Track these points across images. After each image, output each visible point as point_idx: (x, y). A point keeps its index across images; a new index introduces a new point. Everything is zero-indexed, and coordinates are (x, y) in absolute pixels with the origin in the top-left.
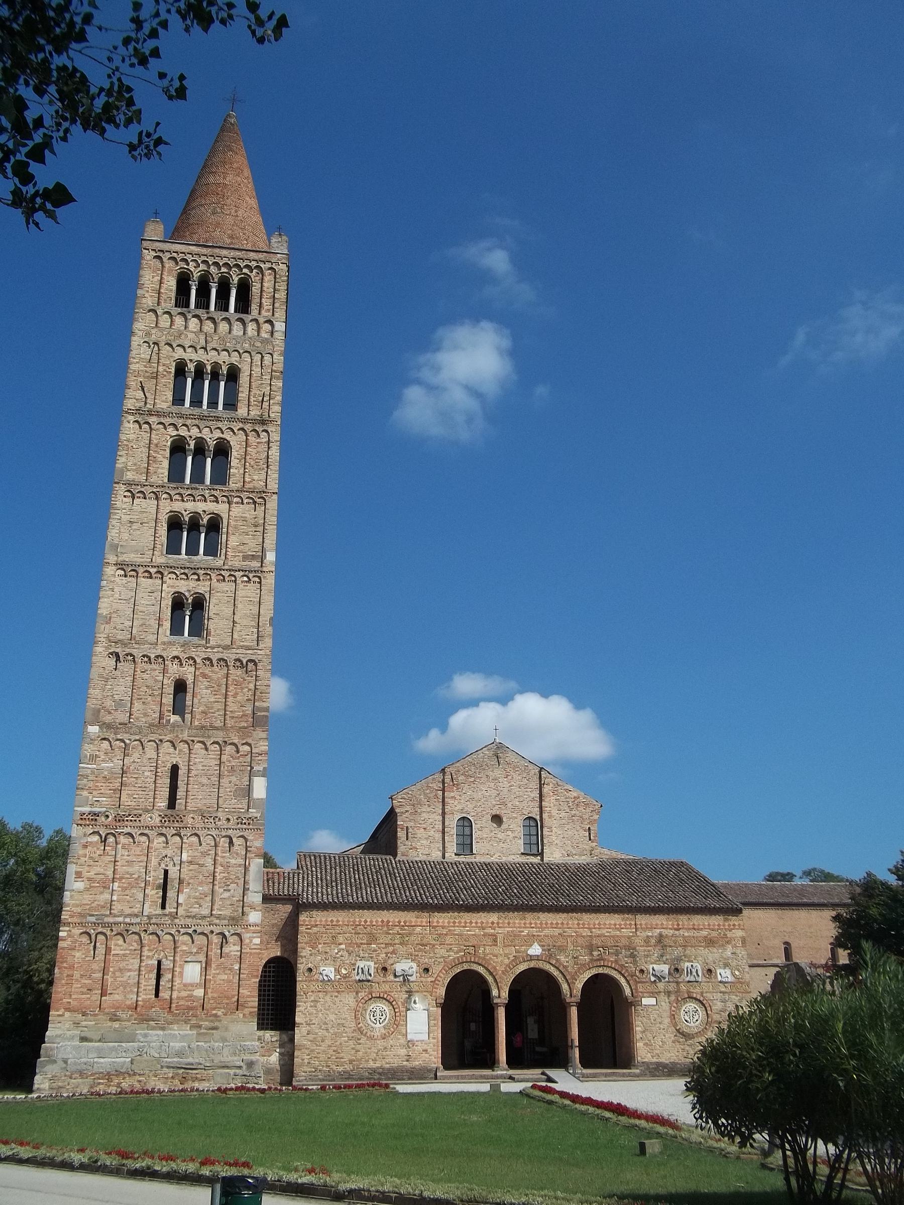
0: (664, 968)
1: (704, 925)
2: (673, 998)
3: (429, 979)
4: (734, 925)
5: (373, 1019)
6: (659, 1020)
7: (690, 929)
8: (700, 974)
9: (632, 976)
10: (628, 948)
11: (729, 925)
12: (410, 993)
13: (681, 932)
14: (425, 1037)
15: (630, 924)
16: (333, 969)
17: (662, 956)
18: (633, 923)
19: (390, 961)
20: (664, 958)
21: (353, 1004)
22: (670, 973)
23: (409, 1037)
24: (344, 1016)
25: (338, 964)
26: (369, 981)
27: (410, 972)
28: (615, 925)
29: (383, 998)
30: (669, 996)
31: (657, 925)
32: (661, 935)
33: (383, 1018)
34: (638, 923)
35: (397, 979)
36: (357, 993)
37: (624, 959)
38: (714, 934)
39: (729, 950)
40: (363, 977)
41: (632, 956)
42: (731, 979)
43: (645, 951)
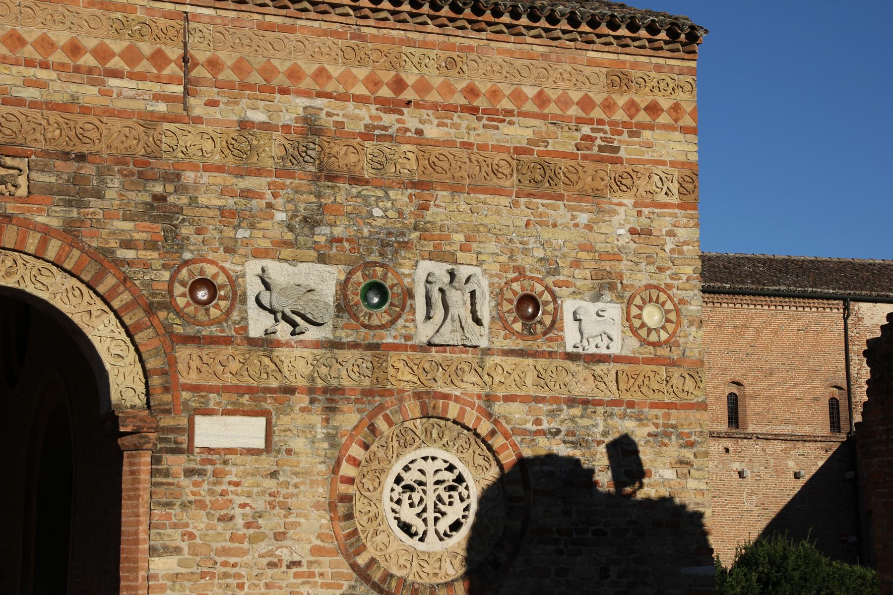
0: (325, 280)
1: (518, 96)
2: (349, 419)
4: (653, 109)
6: (271, 523)
7: (452, 109)
8: (485, 311)
9: (150, 309)
10: (141, 168)
11: (632, 107)
13: (411, 119)
15: (159, 59)
17: (311, 222)
18: (174, 52)
20: (322, 234)
22: (343, 307)
28: (75, 49)
30: (331, 410)
31: (294, 74)
32: (311, 127)
34: (201, 55)
37: (115, 219)
38: (565, 141)
39: (619, 224)
41: (159, 210)
42: (621, 344)
43: (224, 191)
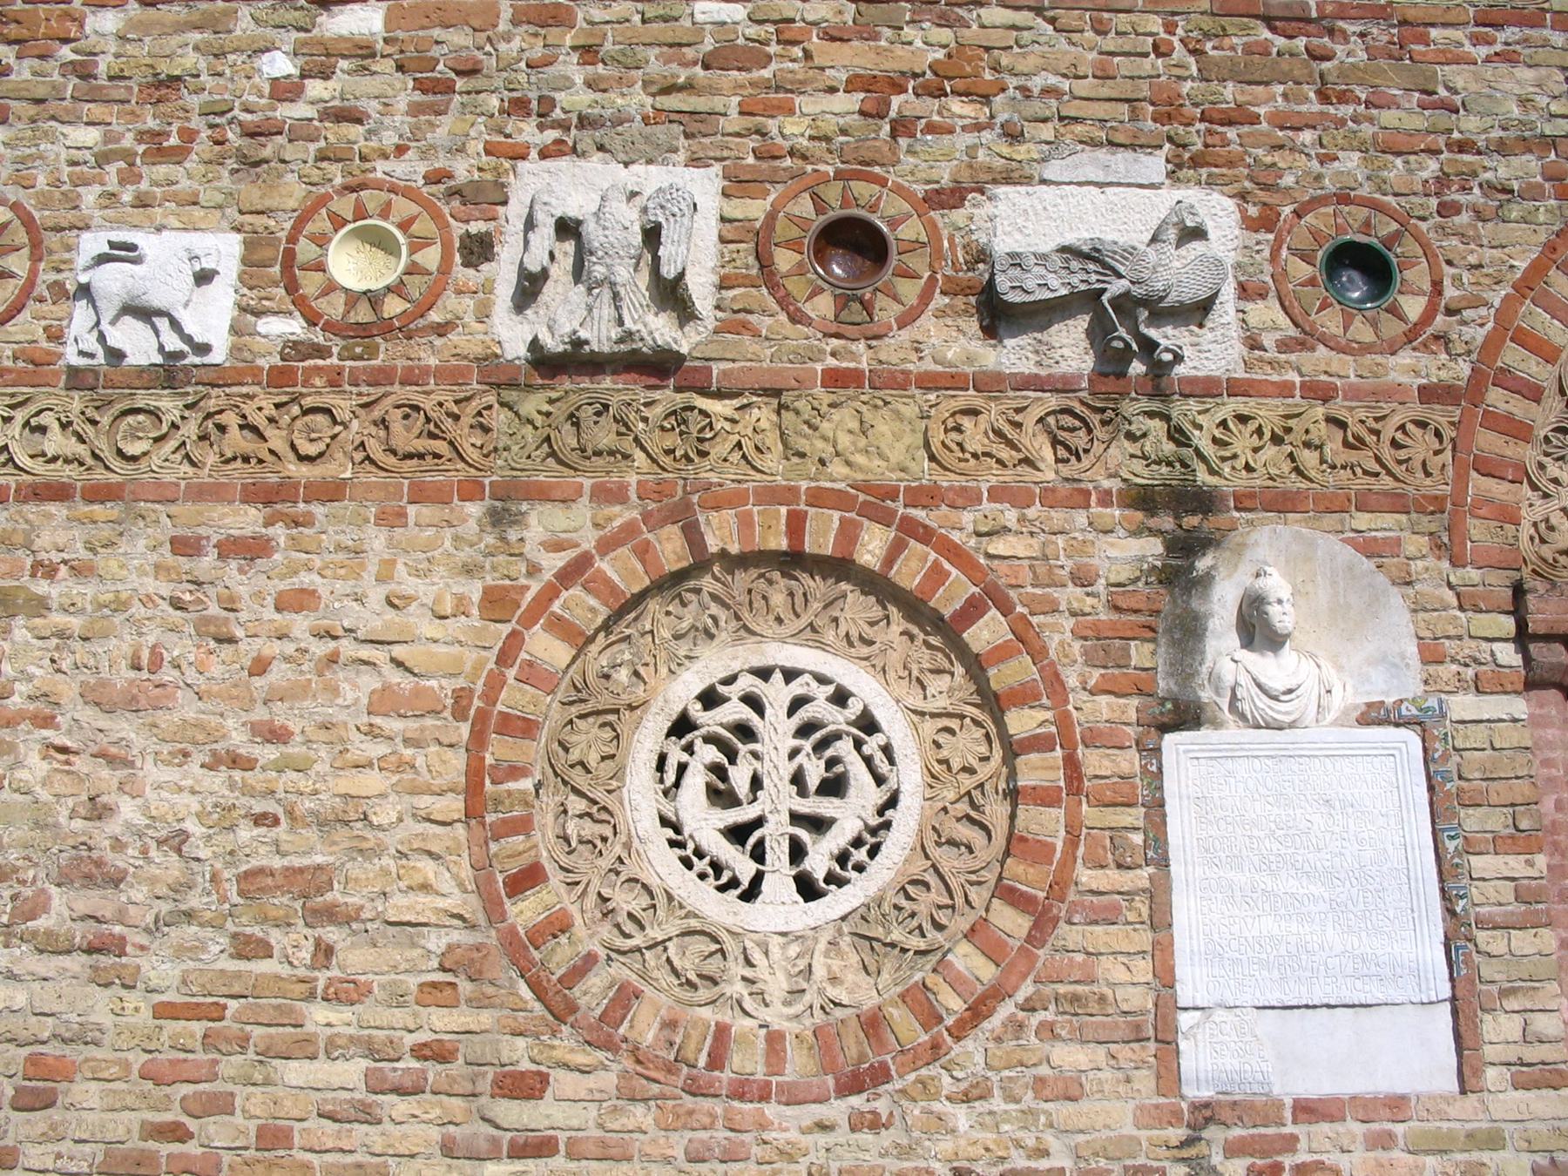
3: (1407, 368)
5: (706, 825)
12: (1187, 519)
14: (1416, 1056)
16: (224, 249)
19: (926, 164)
21: (451, 647)
23: (1209, 1060)
24: (325, 786)
25: (292, 192)
26: (660, 366)
27: (1177, 273)
29: (839, 567)
33: (850, 815)
35: (1014, 355)
36: (499, 519)
40: (566, 316)
